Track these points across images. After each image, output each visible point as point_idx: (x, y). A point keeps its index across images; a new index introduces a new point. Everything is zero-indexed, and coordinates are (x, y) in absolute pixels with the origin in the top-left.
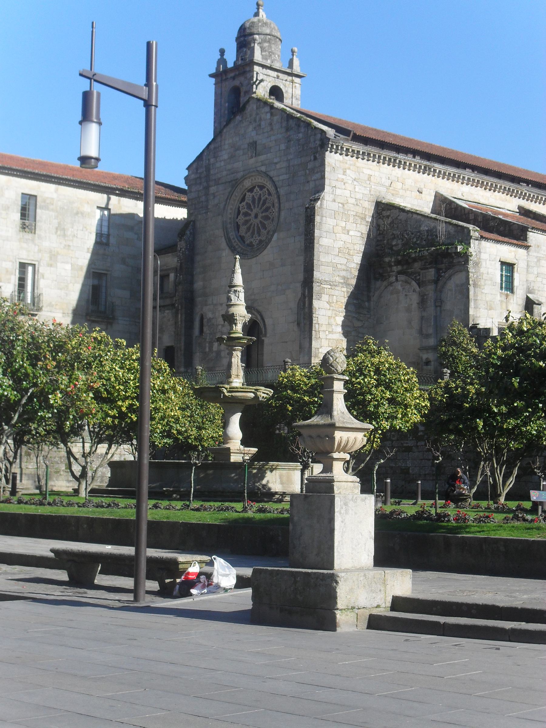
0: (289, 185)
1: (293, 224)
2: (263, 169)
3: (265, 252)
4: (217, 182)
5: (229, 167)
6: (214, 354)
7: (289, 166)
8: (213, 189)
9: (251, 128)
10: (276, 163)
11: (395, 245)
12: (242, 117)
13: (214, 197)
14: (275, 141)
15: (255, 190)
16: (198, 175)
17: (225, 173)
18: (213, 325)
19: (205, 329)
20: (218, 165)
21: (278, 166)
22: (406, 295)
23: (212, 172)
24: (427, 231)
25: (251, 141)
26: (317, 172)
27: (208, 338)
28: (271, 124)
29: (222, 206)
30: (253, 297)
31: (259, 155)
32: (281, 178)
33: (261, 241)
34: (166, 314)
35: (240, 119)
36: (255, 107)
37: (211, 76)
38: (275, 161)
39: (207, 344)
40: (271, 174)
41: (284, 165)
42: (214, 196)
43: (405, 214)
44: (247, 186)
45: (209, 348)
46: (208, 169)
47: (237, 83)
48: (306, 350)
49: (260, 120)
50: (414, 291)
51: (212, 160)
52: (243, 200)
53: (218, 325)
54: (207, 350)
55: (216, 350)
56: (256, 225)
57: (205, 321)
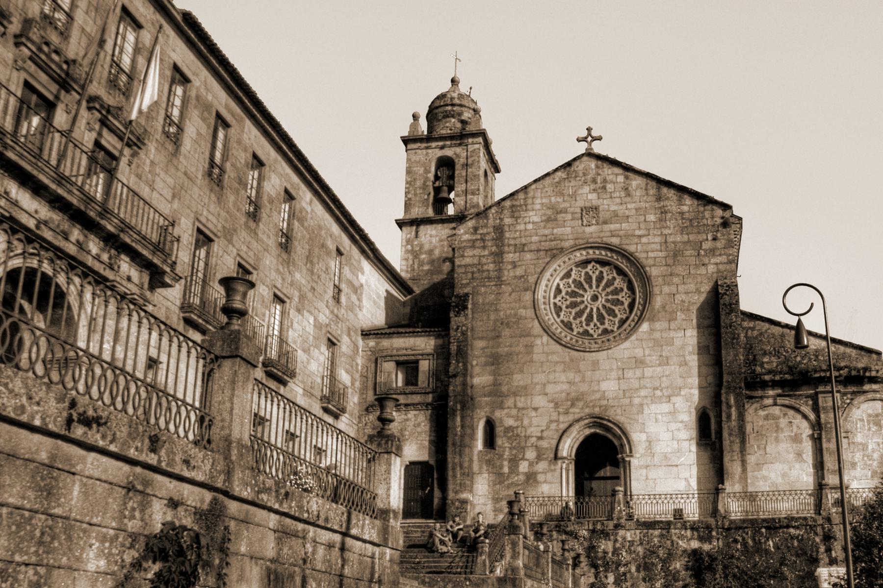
0: (666, 265)
1: (679, 313)
2: (615, 241)
3: (627, 344)
4: (521, 248)
5: (546, 232)
6: (522, 478)
7: (666, 242)
8: (510, 257)
9: (586, 189)
10: (640, 237)
11: (767, 363)
12: (568, 174)
13: (515, 267)
14: (636, 209)
15: (590, 267)
16: (479, 237)
17: (535, 239)
18: (518, 435)
19: (499, 441)
20: (521, 227)
21: (644, 240)
22: (791, 422)
23: (507, 235)
24: (816, 351)
25: (588, 205)
26: (720, 255)
27: (507, 453)
28: (627, 189)
29: (532, 279)
30: (604, 402)
31: (605, 223)
32: (651, 255)
33: (606, 332)
34: (409, 416)
35: (564, 176)
36: (593, 166)
37: (406, 141)
38: (638, 233)
39: (506, 463)
40: (632, 248)
41: (658, 239)
42: (515, 265)
43: (777, 328)
44: (577, 260)
45: (509, 468)
46: (499, 230)
47: (449, 152)
48: (737, 477)
49: (605, 181)
50: (805, 417)
51: (507, 221)
52: (568, 275)
53: (527, 437)
54: (506, 470)
55: (526, 470)
56: (595, 310)
57: (499, 430)
